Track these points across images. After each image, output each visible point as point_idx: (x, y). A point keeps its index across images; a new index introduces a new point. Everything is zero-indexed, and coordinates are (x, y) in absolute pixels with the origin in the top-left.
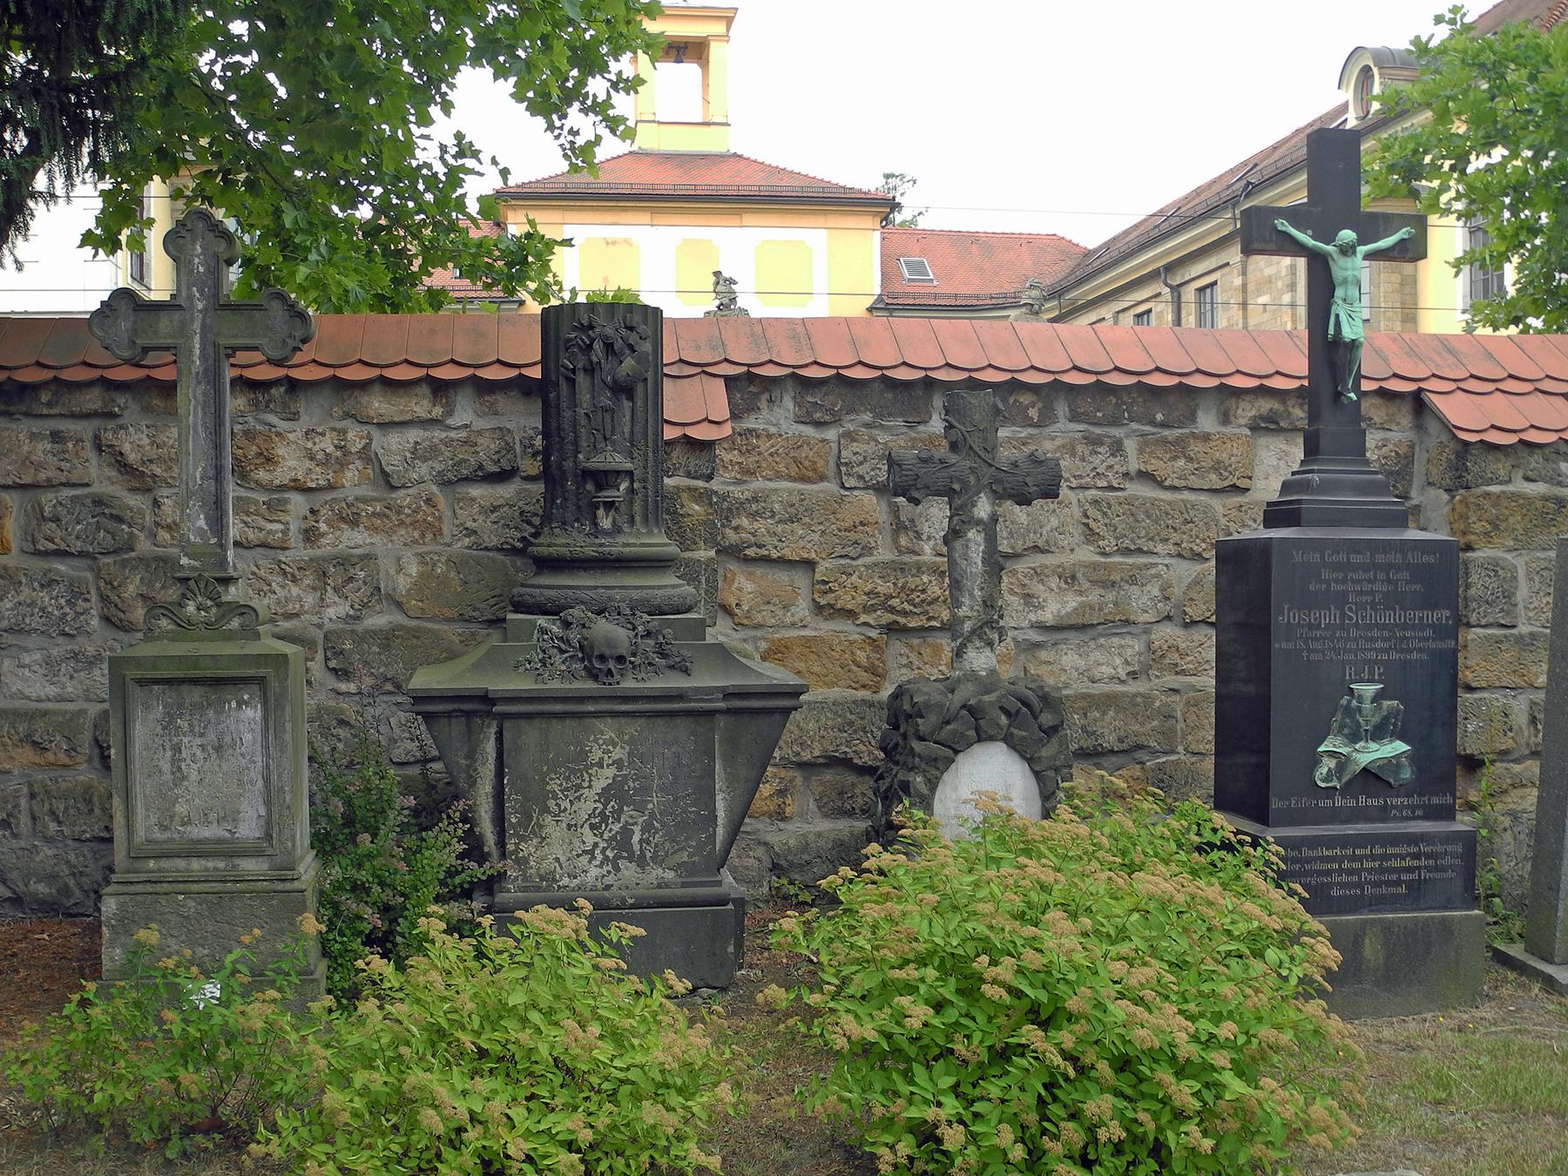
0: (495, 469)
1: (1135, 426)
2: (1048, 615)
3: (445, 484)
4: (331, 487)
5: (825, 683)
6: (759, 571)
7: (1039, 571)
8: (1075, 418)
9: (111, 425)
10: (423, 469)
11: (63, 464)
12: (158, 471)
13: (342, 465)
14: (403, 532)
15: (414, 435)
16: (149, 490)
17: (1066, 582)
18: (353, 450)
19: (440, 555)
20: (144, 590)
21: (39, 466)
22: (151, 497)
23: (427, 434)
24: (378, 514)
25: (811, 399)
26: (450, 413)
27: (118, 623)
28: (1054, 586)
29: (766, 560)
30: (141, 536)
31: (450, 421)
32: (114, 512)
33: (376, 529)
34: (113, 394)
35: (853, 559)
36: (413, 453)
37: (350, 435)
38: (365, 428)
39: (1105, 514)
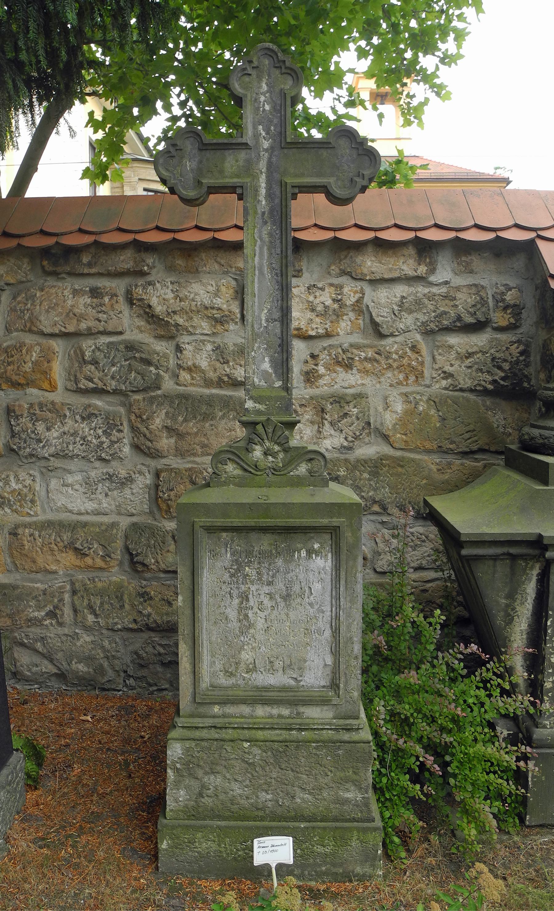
0: (470, 320)
3: (428, 333)
4: (328, 335)
9: (141, 282)
10: (408, 320)
11: (100, 315)
12: (181, 321)
13: (338, 316)
14: (390, 374)
15: (400, 290)
16: (172, 338)
18: (348, 303)
19: (422, 395)
20: (169, 423)
21: (81, 318)
22: (174, 343)
23: (412, 289)
24: (370, 359)
26: (432, 271)
27: (146, 450)
30: (166, 376)
31: (432, 279)
32: (143, 356)
33: (366, 372)
34: (143, 255)
36: (400, 306)
37: (346, 290)
38: (359, 284)
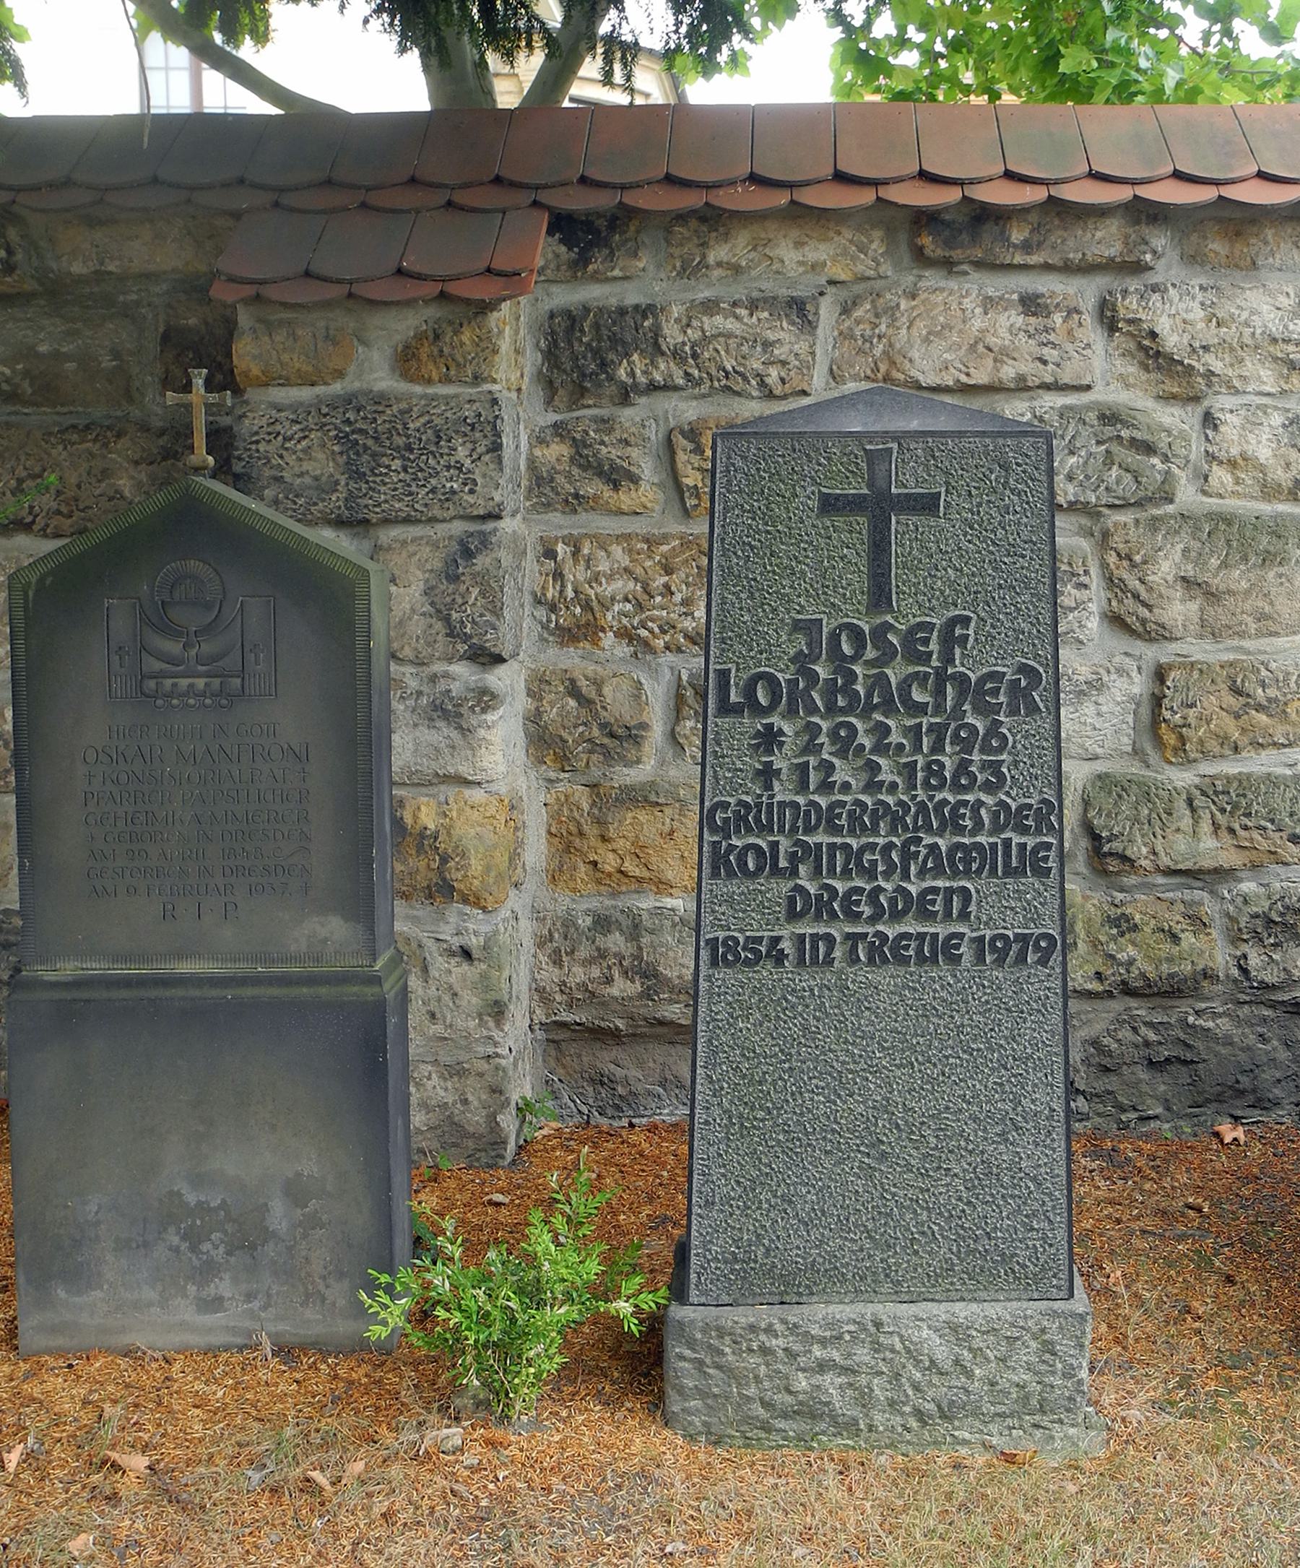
9: (1133, 284)
11: (1046, 351)
12: (1217, 366)
20: (1189, 570)
21: (1002, 355)
27: (1137, 626)
30: (1182, 476)
32: (1138, 435)
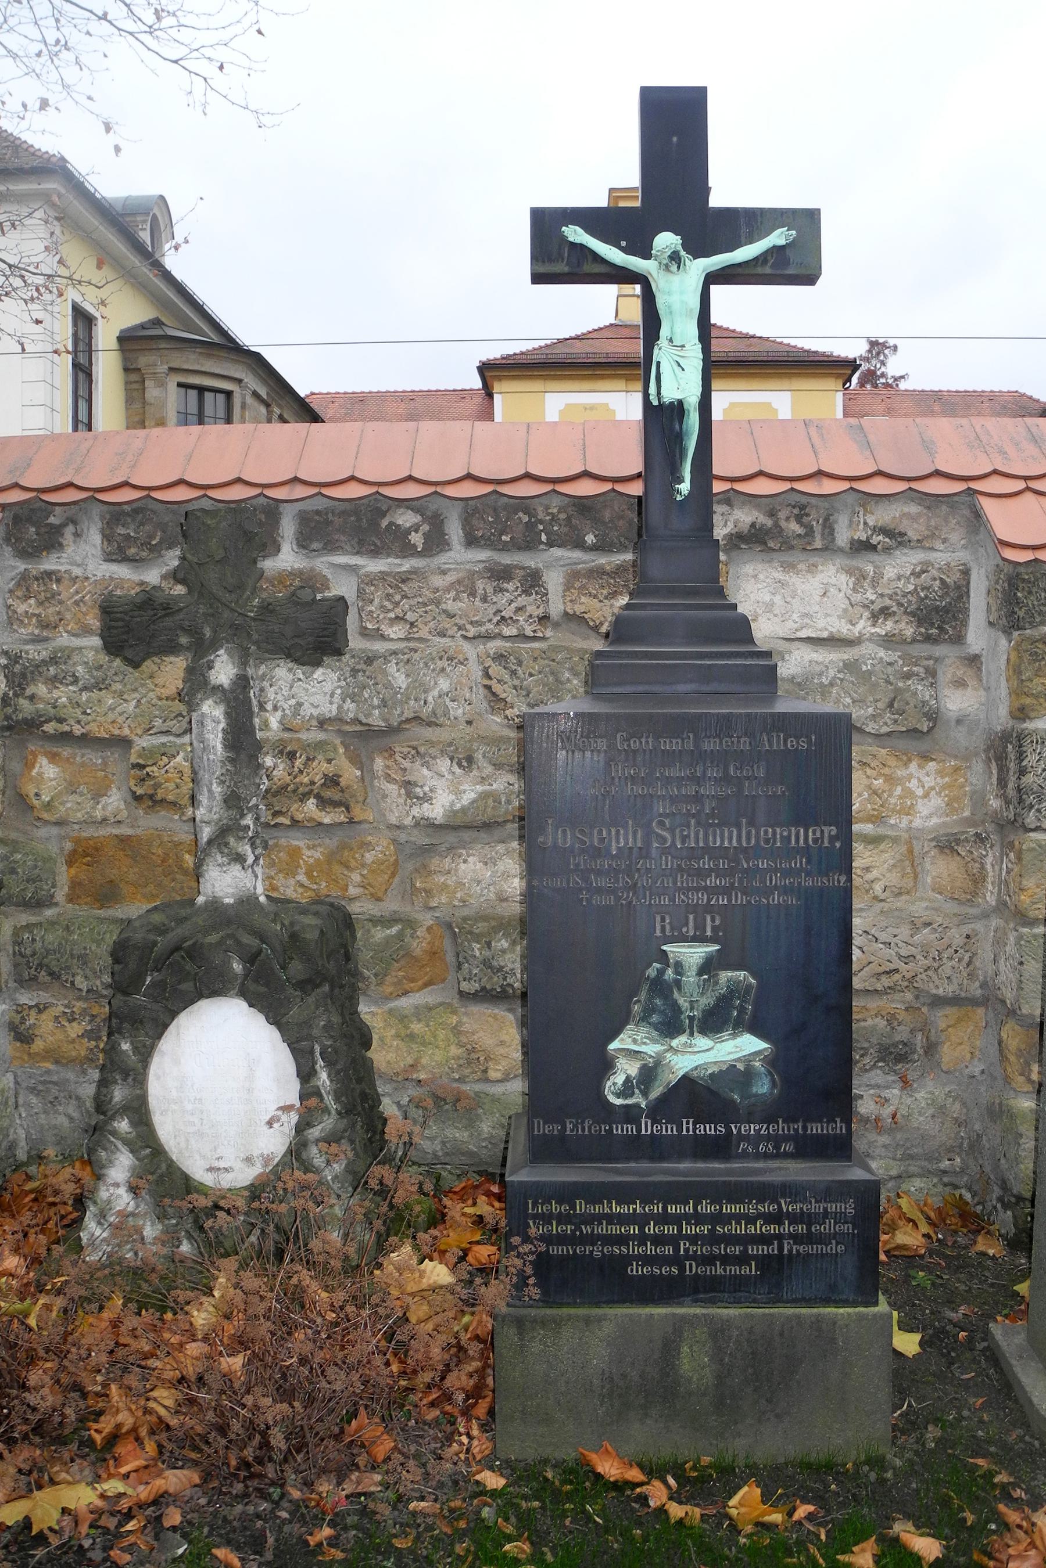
1: (557, 552)
2: (436, 810)
5: (144, 896)
6: (66, 752)
7: (422, 750)
8: (471, 541)
17: (460, 765)
25: (121, 531)
28: (444, 770)
29: (66, 737)
35: (178, 736)
39: (514, 673)
